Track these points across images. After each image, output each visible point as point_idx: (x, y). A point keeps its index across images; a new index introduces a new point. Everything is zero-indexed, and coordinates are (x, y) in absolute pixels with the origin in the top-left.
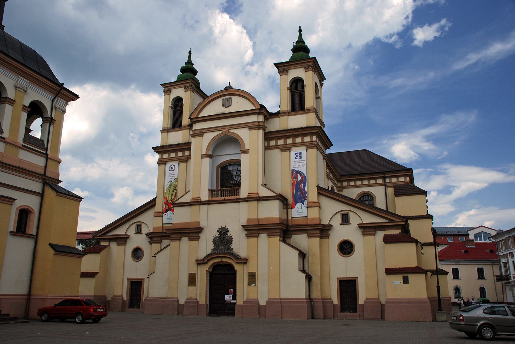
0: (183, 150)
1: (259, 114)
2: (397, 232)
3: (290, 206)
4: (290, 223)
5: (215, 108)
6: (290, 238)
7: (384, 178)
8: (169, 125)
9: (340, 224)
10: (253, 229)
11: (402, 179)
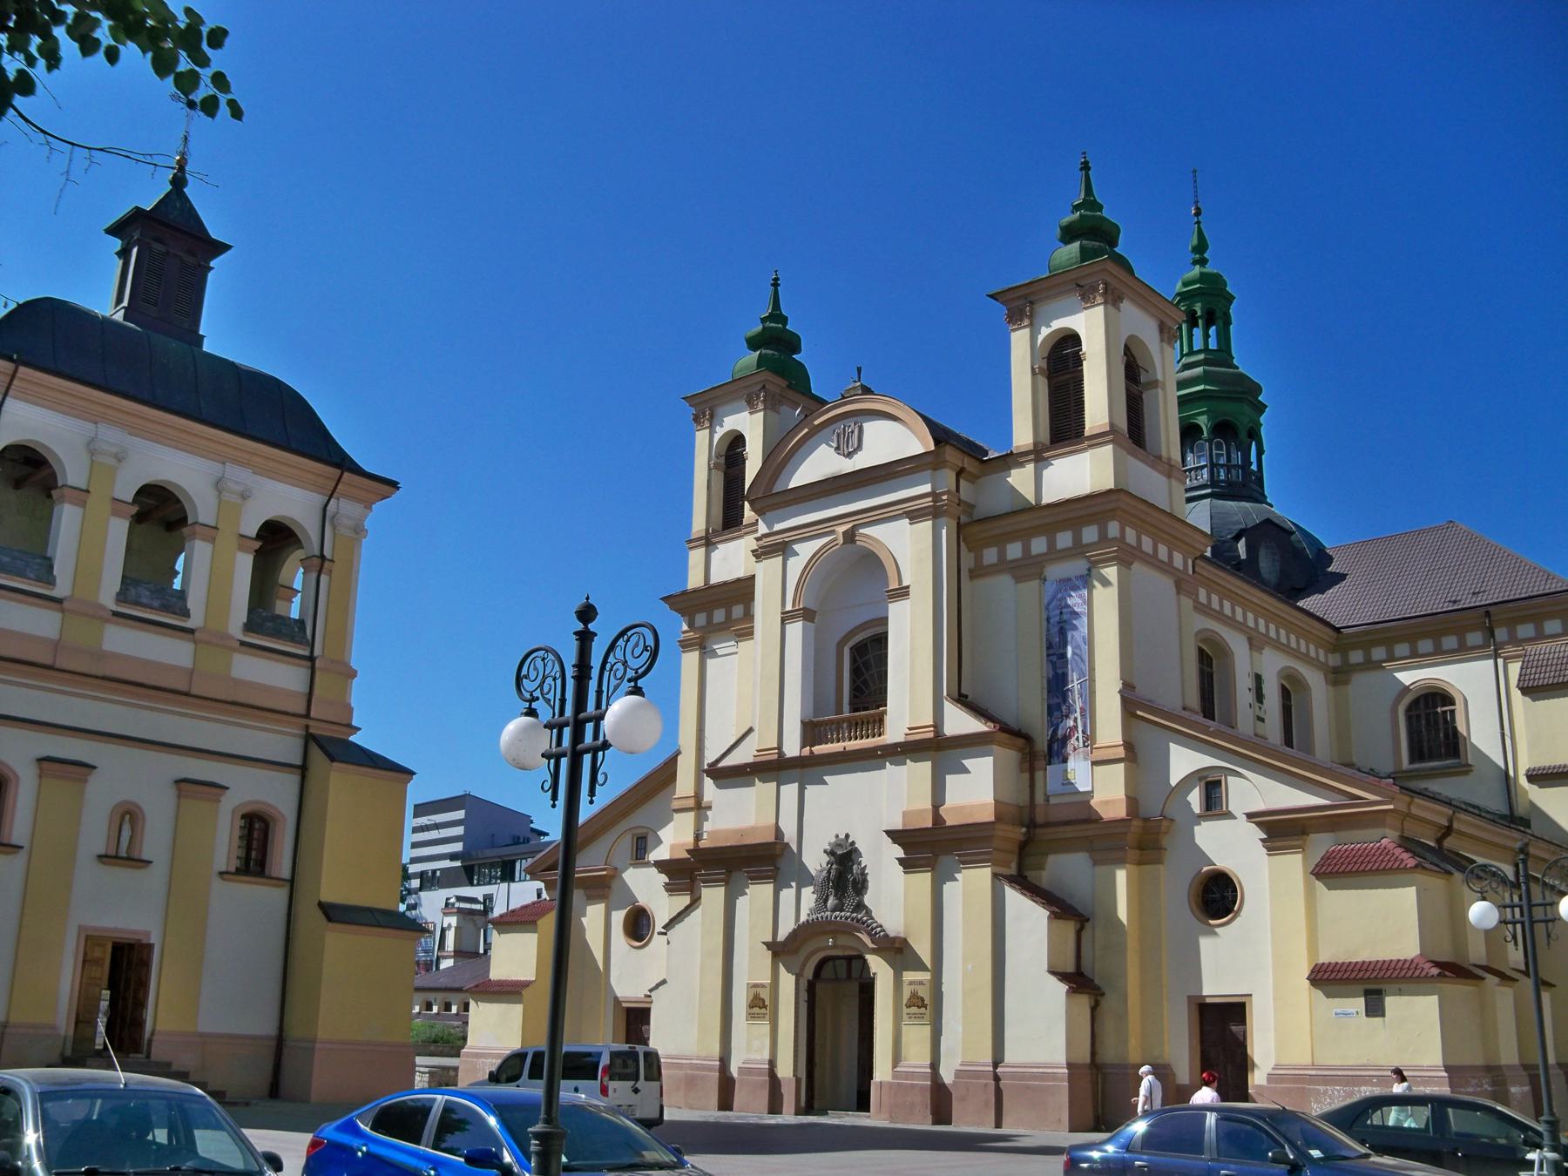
4: (1040, 819)
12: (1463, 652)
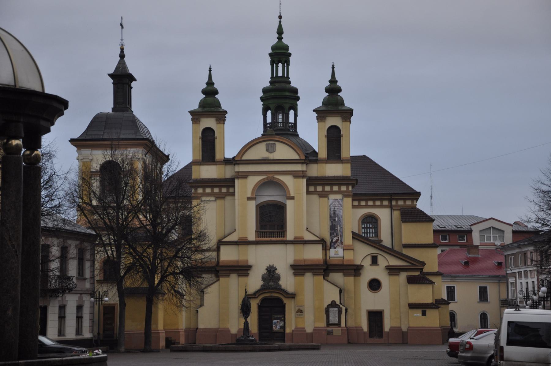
0: (220, 187)
1: (302, 163)
2: (417, 274)
3: (328, 248)
4: (328, 264)
5: (259, 152)
6: (328, 275)
7: (390, 201)
8: (199, 157)
9: (371, 265)
10: (299, 269)
11: (409, 203)
12: (381, 206)
